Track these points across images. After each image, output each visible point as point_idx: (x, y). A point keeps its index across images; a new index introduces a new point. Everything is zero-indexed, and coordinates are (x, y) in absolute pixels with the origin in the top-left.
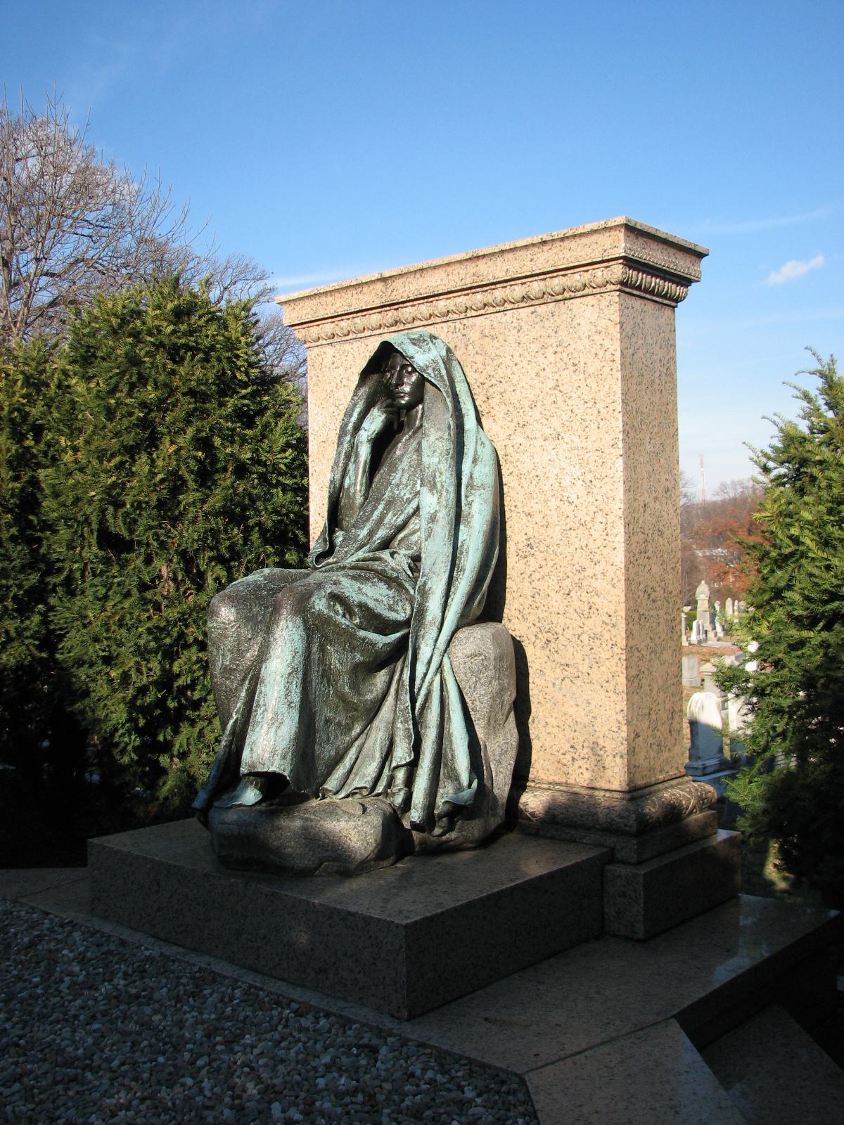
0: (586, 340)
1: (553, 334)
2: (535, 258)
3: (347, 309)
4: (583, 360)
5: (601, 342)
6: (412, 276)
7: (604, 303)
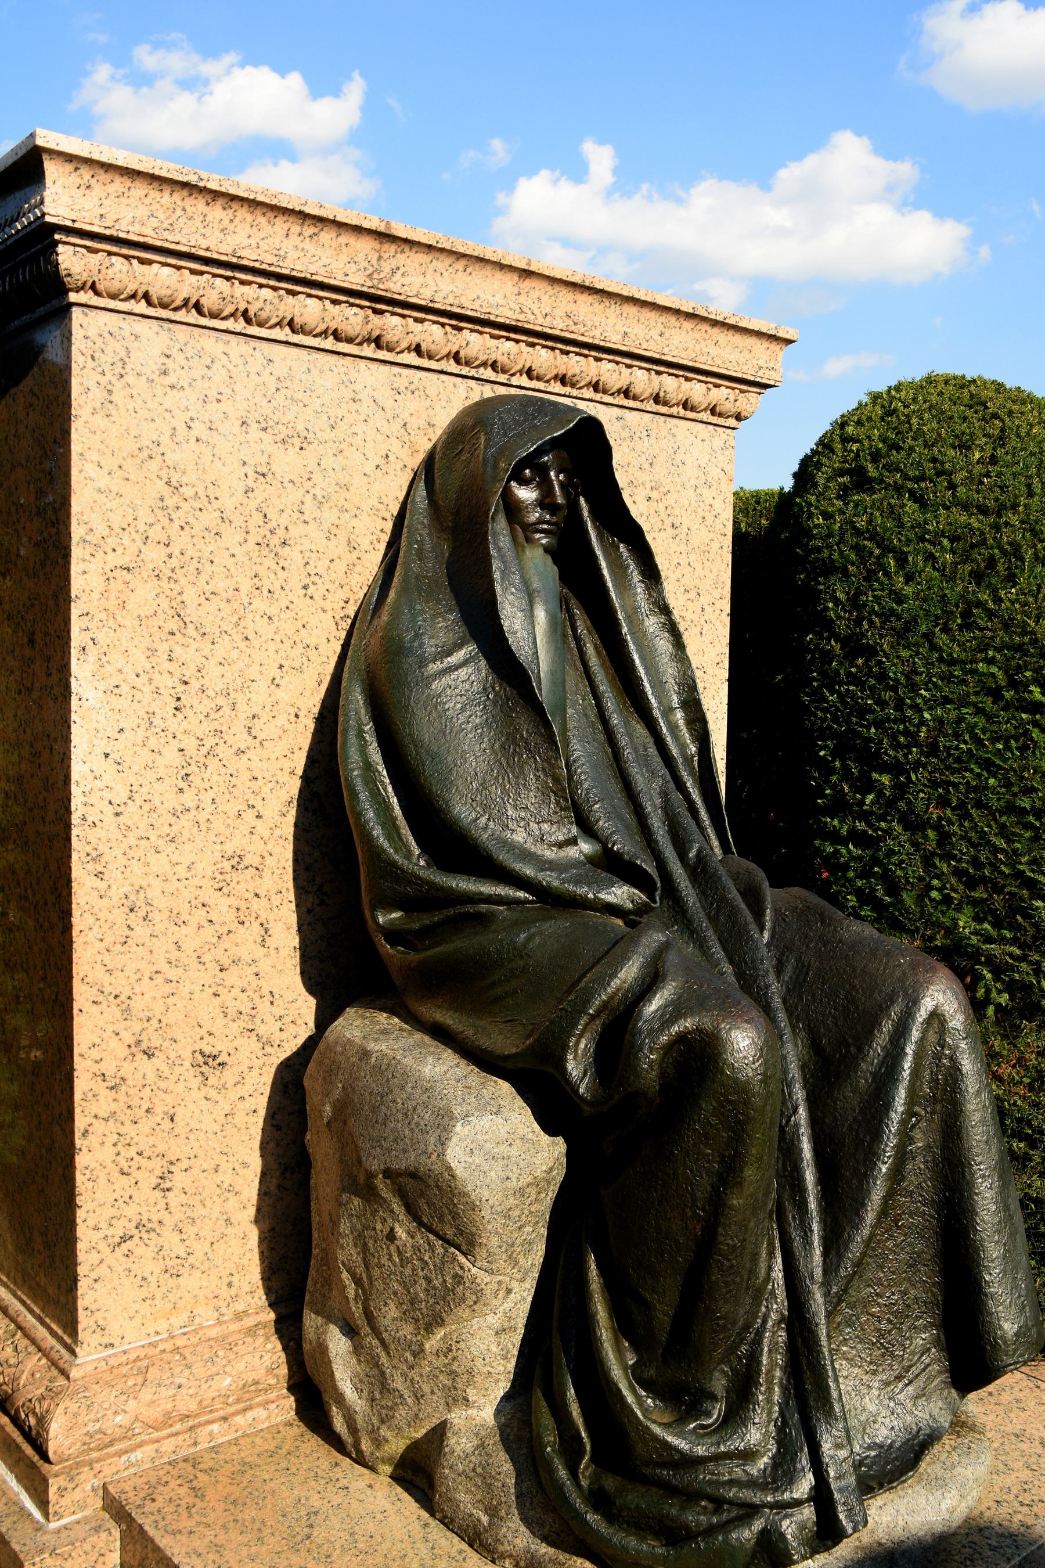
1: (646, 466)
3: (266, 260)
4: (686, 523)
5: (711, 501)
6: (448, 260)
7: (718, 443)
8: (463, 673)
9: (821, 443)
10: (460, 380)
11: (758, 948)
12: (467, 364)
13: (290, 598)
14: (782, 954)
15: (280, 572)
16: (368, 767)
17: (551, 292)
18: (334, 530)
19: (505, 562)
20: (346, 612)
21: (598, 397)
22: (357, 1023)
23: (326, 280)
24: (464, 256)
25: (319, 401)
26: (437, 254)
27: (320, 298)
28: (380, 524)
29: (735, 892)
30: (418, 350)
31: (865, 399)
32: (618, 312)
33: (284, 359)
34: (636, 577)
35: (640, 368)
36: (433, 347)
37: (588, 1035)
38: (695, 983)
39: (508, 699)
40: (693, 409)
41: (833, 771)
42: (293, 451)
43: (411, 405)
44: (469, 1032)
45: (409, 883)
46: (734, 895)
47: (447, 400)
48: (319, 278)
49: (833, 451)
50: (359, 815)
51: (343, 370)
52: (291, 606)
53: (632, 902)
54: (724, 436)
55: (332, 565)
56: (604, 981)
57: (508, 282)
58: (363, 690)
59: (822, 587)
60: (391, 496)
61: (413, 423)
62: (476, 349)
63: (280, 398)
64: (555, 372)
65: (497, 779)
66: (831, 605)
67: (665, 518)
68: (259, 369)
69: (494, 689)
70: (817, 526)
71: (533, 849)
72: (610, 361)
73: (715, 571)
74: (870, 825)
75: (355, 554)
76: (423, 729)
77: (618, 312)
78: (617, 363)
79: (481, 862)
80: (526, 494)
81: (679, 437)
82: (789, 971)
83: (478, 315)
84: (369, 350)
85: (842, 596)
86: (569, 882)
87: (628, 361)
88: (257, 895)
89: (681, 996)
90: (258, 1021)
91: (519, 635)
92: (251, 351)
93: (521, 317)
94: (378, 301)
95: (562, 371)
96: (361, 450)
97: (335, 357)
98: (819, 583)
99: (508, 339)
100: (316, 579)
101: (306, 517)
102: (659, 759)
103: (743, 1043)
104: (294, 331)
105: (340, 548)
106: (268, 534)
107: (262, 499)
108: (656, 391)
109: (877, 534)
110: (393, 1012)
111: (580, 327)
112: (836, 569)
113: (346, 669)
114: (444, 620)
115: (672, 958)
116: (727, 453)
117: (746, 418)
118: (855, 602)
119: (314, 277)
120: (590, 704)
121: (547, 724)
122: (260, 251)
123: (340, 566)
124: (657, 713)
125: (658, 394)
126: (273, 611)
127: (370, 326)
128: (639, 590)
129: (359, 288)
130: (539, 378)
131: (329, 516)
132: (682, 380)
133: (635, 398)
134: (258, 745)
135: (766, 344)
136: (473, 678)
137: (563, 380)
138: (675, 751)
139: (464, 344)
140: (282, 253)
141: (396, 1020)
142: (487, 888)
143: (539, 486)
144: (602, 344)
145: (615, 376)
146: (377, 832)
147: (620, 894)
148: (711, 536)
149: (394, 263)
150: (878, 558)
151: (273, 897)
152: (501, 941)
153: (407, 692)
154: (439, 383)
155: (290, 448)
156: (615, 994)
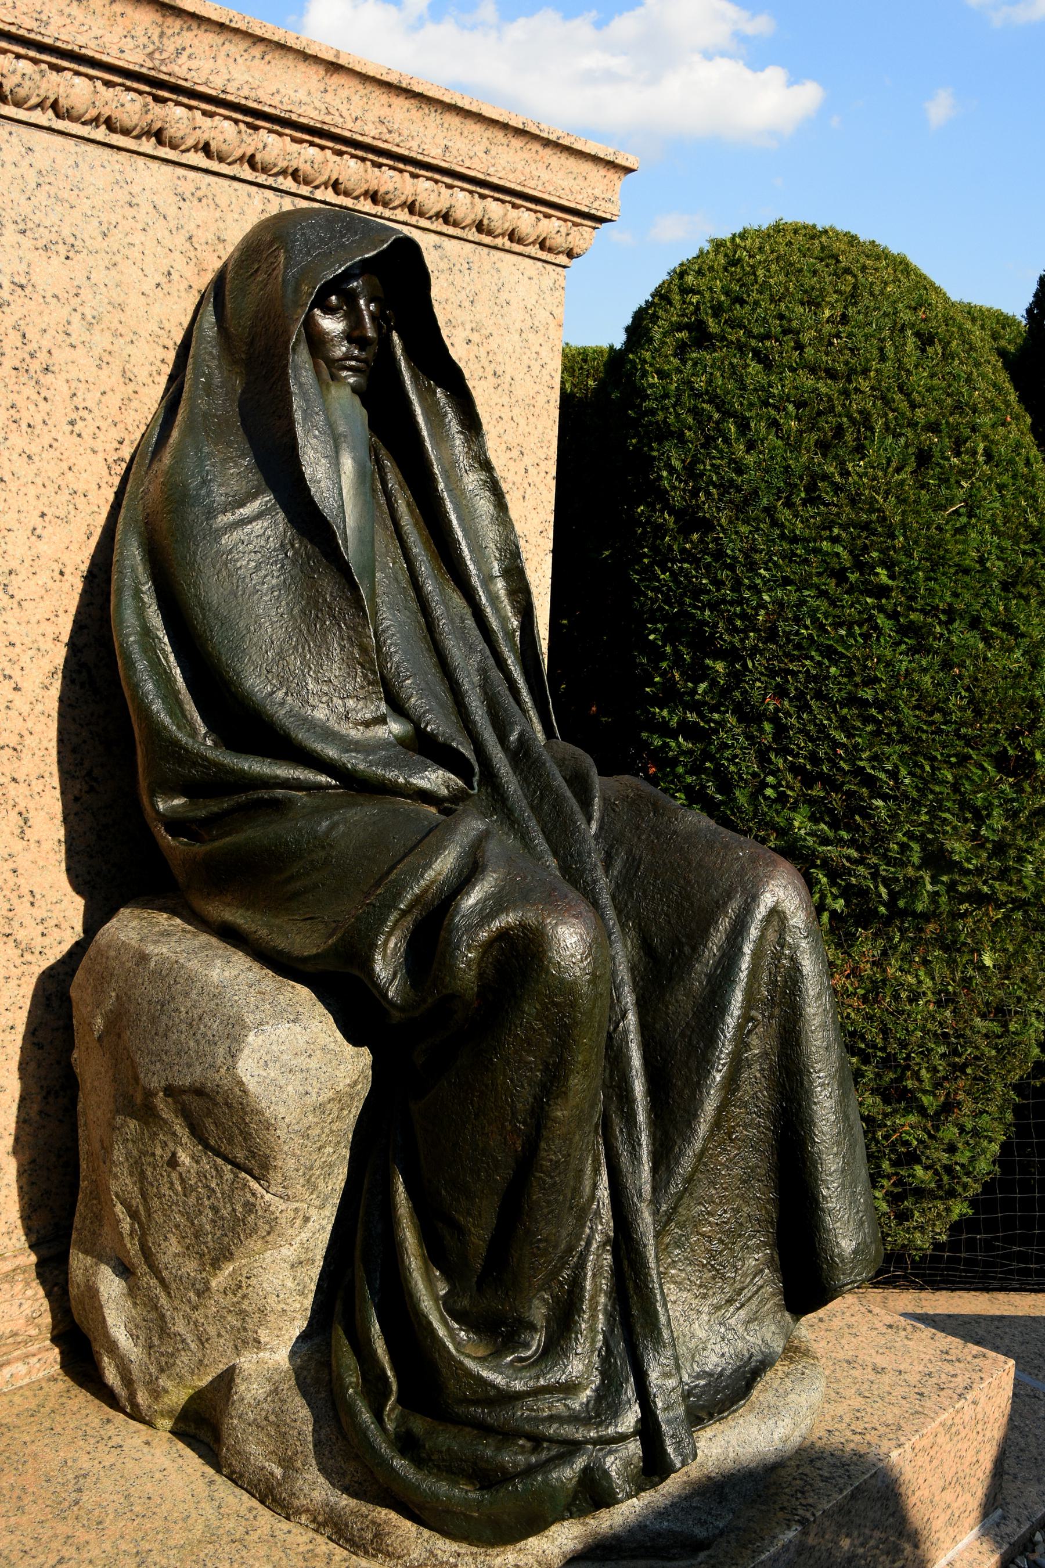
0: (516, 336)
1: (467, 304)
2: (494, 151)
5: (537, 348)
6: (243, 45)
7: (547, 282)
8: (257, 527)
9: (657, 293)
10: (255, 189)
11: (585, 841)
12: (264, 170)
13: (54, 434)
14: (612, 847)
15: (42, 404)
16: (147, 632)
17: (362, 92)
18: (106, 358)
19: (307, 401)
20: (120, 454)
21: (414, 220)
22: (133, 925)
23: (97, 56)
24: (262, 40)
25: (89, 202)
26: (230, 36)
27: (91, 78)
28: (161, 353)
29: (561, 779)
30: (206, 149)
31: (707, 247)
32: (439, 121)
33: (47, 149)
34: (454, 427)
35: (462, 189)
36: (224, 148)
37: (398, 933)
38: (518, 875)
39: (309, 558)
40: (520, 241)
41: (663, 657)
42: (56, 261)
43: (198, 215)
44: (263, 932)
45: (194, 764)
46: (559, 781)
47: (239, 212)
48: (90, 53)
49: (670, 303)
50: (136, 687)
51: (118, 167)
52: (55, 444)
53: (448, 787)
54: (553, 275)
55: (104, 399)
56: (416, 873)
57: (314, 75)
58: (141, 545)
59: (655, 454)
60: (174, 321)
61: (200, 236)
62: (275, 152)
63: (41, 196)
64: (365, 187)
65: (295, 648)
66: (665, 474)
67: (486, 364)
68: (17, 158)
69: (293, 546)
70: (652, 386)
71: (336, 727)
72: (428, 179)
73: (540, 427)
74: (701, 715)
75: (132, 387)
76: (211, 589)
77: (439, 121)
78: (436, 182)
79: (278, 743)
80: (332, 325)
81: (504, 273)
82: (618, 865)
83: (277, 112)
84: (148, 146)
85: (676, 463)
86: (377, 765)
87: (448, 180)
88: (14, 780)
89: (503, 888)
90: (15, 924)
91: (322, 484)
92: (7, 136)
93: (328, 119)
94: (160, 87)
95: (373, 186)
96: (139, 264)
97: (108, 151)
98: (652, 449)
99: (312, 144)
100: (85, 414)
101: (72, 340)
102: (477, 632)
103: (569, 940)
104: (58, 116)
105: (113, 379)
106: (27, 357)
107: (19, 315)
108: (479, 217)
109: (717, 396)
110: (174, 912)
111: (395, 135)
112: (672, 434)
113: (120, 520)
114: (236, 465)
115: (492, 848)
116: (557, 294)
117: (579, 255)
118: (691, 471)
119: (83, 51)
120: (402, 568)
121: (354, 587)
122: (16, 12)
123: (113, 401)
124: (475, 581)
125: (481, 221)
126: (33, 449)
127: (150, 117)
128: (458, 442)
129: (137, 68)
130: (347, 194)
131: (101, 340)
132: (509, 206)
133: (456, 224)
134: (15, 606)
135: (603, 171)
136: (269, 532)
137: (374, 197)
138: (495, 624)
139: (261, 146)
140: (45, 18)
141: (178, 921)
142: (284, 771)
143: (346, 316)
144: (420, 157)
145: (434, 197)
146: (157, 706)
147: (434, 779)
148: (537, 388)
149: (179, 41)
150: (717, 423)
151: (34, 782)
152: (300, 830)
153: (192, 547)
154: (231, 191)
155: (54, 256)
156: (429, 887)
